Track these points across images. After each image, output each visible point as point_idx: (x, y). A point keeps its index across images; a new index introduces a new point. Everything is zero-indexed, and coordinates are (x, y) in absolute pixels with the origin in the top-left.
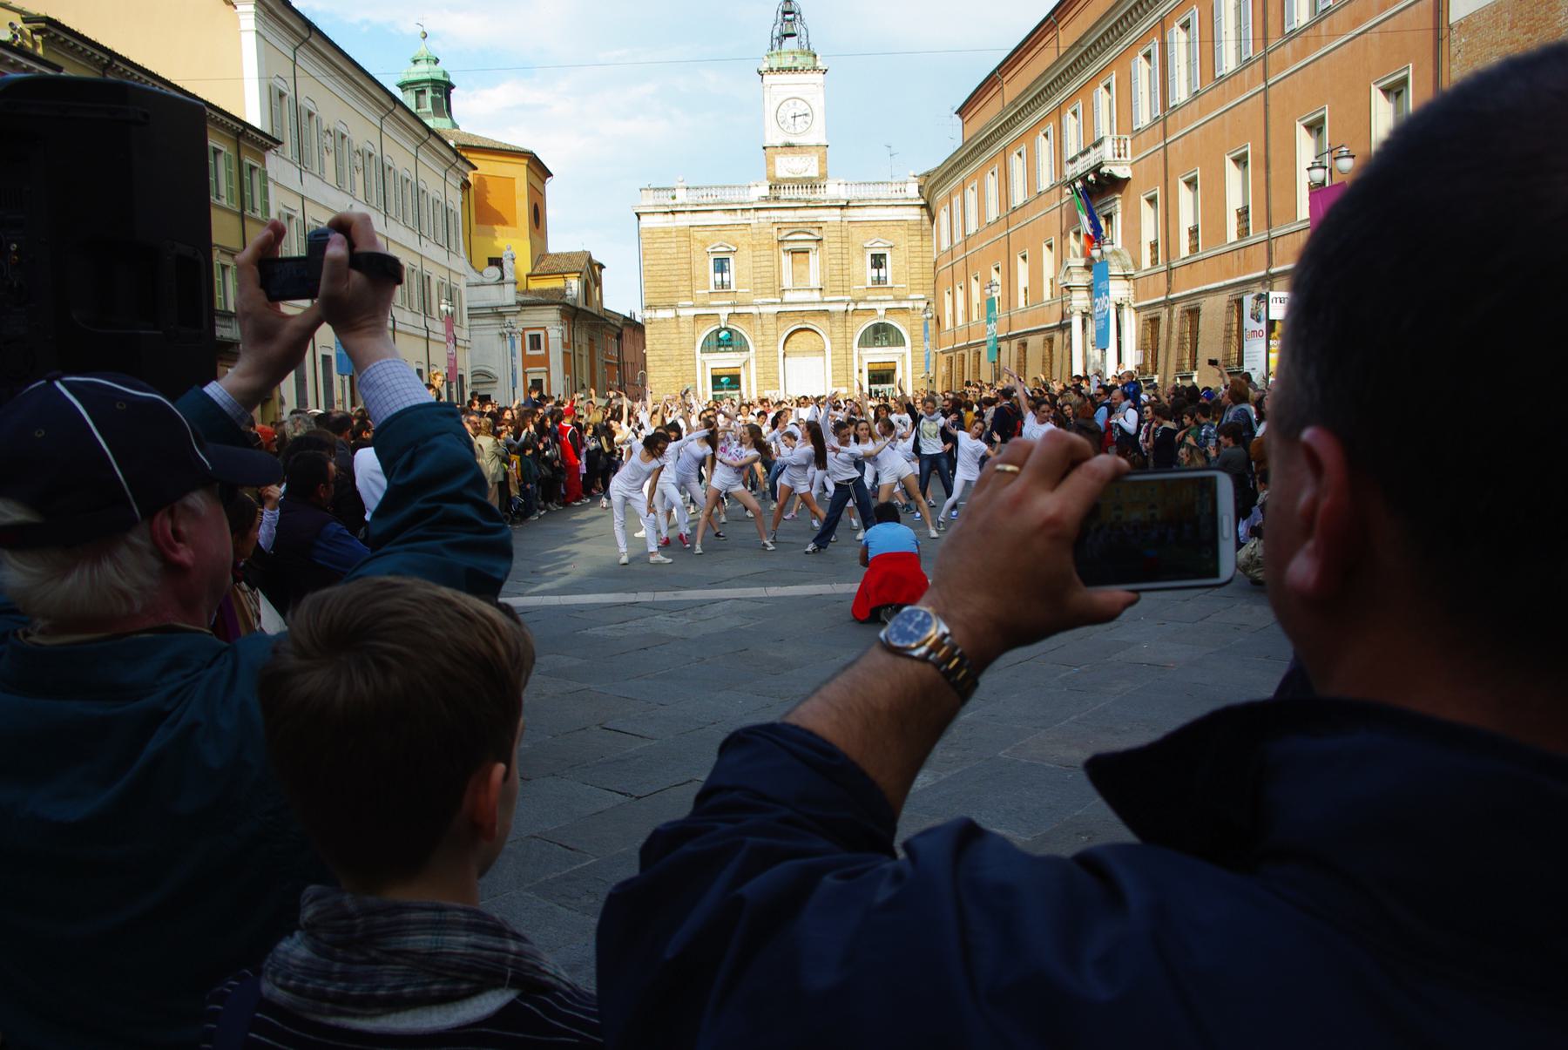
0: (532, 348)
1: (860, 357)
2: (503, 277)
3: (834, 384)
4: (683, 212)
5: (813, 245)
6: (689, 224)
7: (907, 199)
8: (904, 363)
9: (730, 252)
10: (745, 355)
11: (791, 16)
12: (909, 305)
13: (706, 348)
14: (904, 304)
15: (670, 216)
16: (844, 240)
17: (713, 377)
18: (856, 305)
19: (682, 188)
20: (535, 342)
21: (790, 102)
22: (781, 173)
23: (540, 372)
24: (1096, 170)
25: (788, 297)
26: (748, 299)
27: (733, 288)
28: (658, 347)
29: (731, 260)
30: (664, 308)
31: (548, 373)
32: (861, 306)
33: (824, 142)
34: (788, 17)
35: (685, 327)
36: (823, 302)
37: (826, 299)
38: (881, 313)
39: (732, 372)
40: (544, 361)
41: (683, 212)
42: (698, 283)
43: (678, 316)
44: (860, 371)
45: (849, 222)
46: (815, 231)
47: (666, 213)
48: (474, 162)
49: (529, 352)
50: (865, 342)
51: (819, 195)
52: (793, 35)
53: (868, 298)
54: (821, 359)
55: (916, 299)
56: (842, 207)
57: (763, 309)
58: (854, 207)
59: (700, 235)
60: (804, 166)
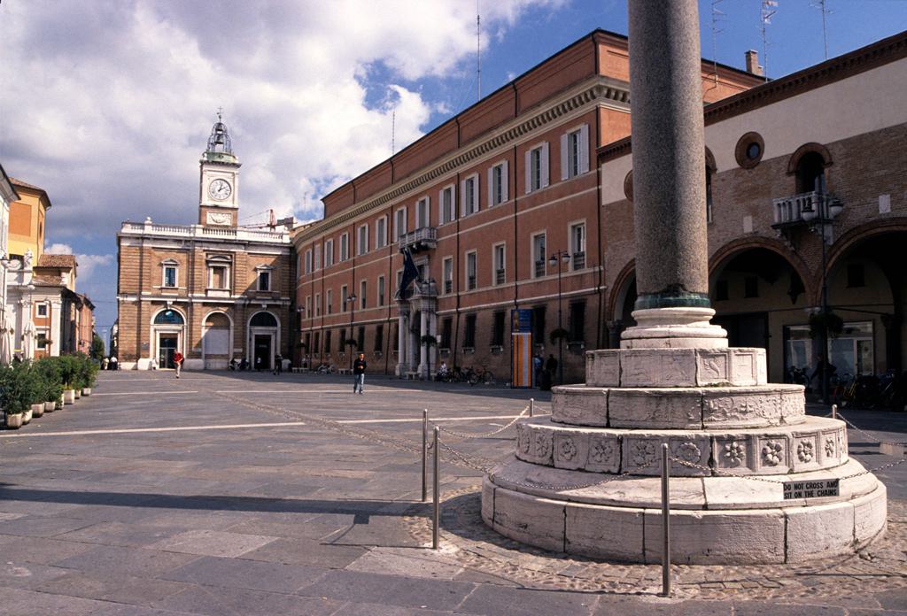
0: (40, 313)
1: (251, 331)
2: (22, 268)
3: (235, 347)
4: (149, 239)
5: (227, 266)
6: (151, 246)
7: (282, 243)
8: (276, 336)
9: (176, 265)
10: (180, 328)
11: (220, 133)
12: (281, 303)
13: (157, 321)
14: (278, 303)
15: (140, 241)
16: (246, 263)
17: (161, 339)
18: (250, 300)
19: (149, 225)
20: (42, 310)
21: (218, 181)
22: (209, 222)
23: (46, 330)
24: (418, 243)
25: (211, 294)
26: (184, 293)
27: (176, 286)
28: (126, 318)
29: (177, 271)
30: (132, 295)
31: (50, 330)
32: (252, 302)
33: (236, 206)
34: (219, 132)
35: (144, 306)
36: (230, 299)
37: (232, 296)
38: (265, 306)
39: (173, 337)
40: (49, 322)
41: (149, 239)
42: (155, 281)
43: (141, 301)
44: (250, 339)
45: (249, 254)
46: (229, 257)
47: (138, 238)
48: (20, 196)
49: (38, 316)
50: (252, 324)
51: (232, 237)
52: (221, 143)
53: (258, 297)
54: (227, 331)
55: (285, 300)
56: (244, 245)
57: (193, 300)
58: (252, 245)
59: (158, 253)
60: (225, 219)
